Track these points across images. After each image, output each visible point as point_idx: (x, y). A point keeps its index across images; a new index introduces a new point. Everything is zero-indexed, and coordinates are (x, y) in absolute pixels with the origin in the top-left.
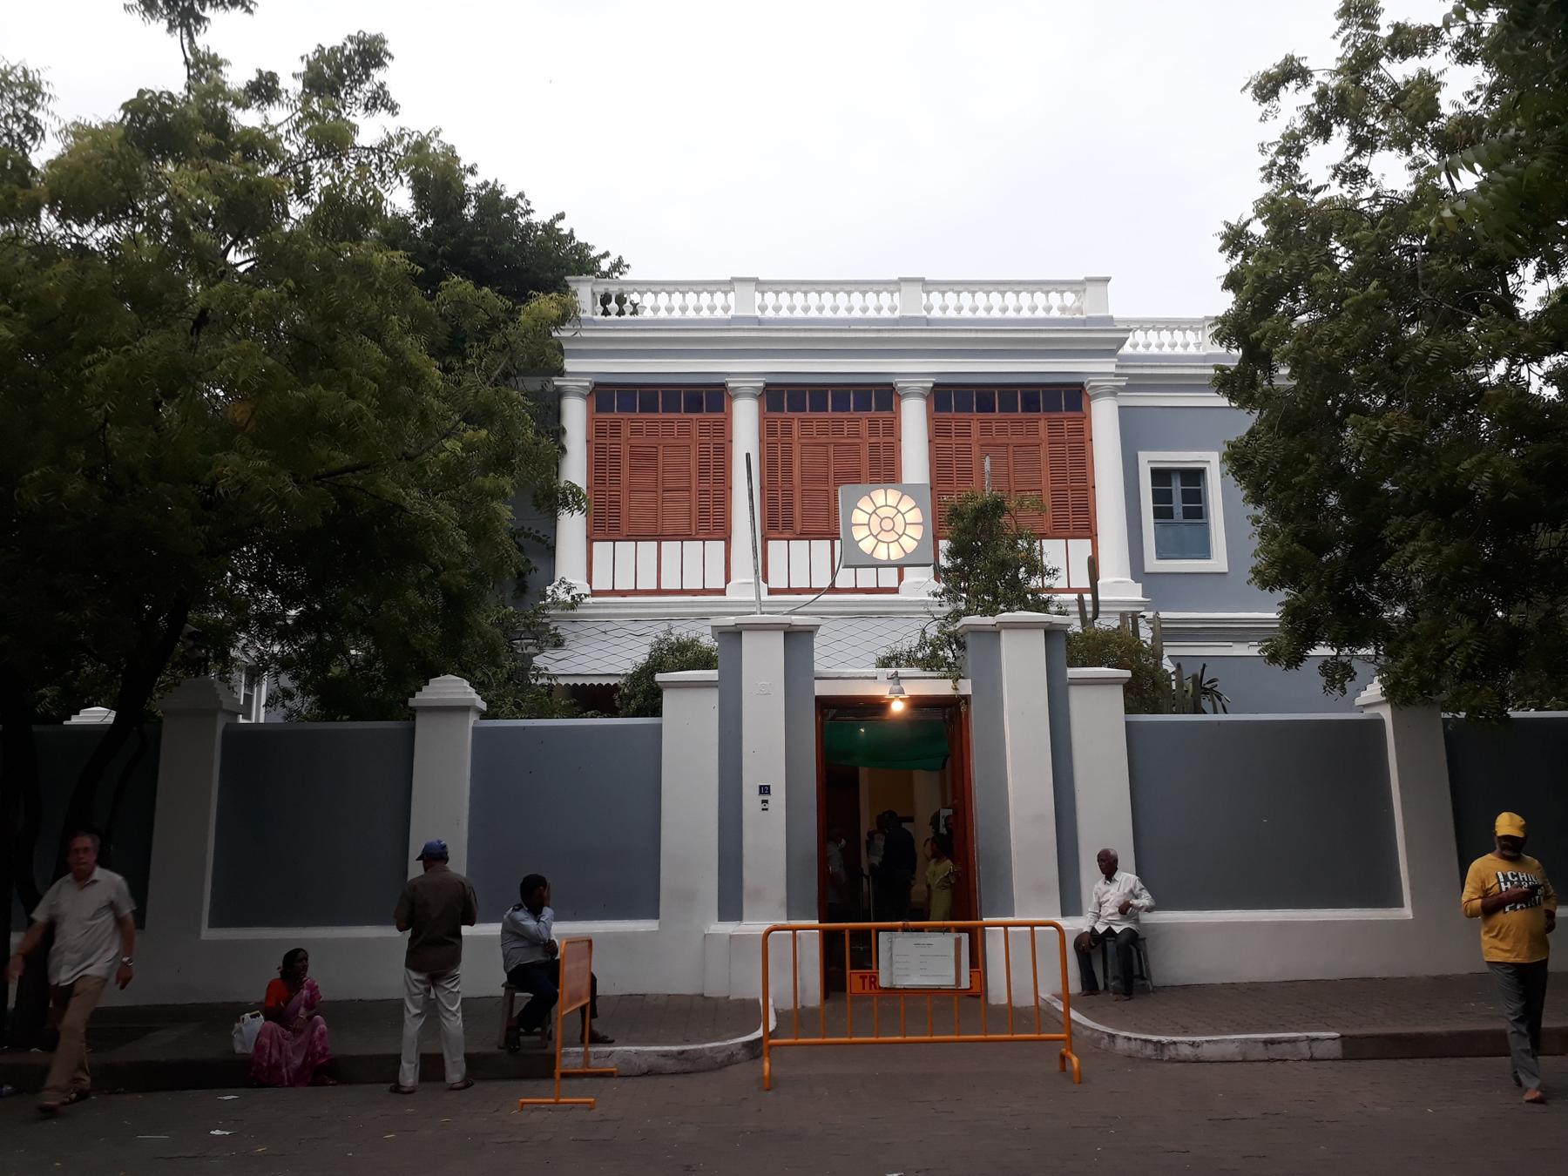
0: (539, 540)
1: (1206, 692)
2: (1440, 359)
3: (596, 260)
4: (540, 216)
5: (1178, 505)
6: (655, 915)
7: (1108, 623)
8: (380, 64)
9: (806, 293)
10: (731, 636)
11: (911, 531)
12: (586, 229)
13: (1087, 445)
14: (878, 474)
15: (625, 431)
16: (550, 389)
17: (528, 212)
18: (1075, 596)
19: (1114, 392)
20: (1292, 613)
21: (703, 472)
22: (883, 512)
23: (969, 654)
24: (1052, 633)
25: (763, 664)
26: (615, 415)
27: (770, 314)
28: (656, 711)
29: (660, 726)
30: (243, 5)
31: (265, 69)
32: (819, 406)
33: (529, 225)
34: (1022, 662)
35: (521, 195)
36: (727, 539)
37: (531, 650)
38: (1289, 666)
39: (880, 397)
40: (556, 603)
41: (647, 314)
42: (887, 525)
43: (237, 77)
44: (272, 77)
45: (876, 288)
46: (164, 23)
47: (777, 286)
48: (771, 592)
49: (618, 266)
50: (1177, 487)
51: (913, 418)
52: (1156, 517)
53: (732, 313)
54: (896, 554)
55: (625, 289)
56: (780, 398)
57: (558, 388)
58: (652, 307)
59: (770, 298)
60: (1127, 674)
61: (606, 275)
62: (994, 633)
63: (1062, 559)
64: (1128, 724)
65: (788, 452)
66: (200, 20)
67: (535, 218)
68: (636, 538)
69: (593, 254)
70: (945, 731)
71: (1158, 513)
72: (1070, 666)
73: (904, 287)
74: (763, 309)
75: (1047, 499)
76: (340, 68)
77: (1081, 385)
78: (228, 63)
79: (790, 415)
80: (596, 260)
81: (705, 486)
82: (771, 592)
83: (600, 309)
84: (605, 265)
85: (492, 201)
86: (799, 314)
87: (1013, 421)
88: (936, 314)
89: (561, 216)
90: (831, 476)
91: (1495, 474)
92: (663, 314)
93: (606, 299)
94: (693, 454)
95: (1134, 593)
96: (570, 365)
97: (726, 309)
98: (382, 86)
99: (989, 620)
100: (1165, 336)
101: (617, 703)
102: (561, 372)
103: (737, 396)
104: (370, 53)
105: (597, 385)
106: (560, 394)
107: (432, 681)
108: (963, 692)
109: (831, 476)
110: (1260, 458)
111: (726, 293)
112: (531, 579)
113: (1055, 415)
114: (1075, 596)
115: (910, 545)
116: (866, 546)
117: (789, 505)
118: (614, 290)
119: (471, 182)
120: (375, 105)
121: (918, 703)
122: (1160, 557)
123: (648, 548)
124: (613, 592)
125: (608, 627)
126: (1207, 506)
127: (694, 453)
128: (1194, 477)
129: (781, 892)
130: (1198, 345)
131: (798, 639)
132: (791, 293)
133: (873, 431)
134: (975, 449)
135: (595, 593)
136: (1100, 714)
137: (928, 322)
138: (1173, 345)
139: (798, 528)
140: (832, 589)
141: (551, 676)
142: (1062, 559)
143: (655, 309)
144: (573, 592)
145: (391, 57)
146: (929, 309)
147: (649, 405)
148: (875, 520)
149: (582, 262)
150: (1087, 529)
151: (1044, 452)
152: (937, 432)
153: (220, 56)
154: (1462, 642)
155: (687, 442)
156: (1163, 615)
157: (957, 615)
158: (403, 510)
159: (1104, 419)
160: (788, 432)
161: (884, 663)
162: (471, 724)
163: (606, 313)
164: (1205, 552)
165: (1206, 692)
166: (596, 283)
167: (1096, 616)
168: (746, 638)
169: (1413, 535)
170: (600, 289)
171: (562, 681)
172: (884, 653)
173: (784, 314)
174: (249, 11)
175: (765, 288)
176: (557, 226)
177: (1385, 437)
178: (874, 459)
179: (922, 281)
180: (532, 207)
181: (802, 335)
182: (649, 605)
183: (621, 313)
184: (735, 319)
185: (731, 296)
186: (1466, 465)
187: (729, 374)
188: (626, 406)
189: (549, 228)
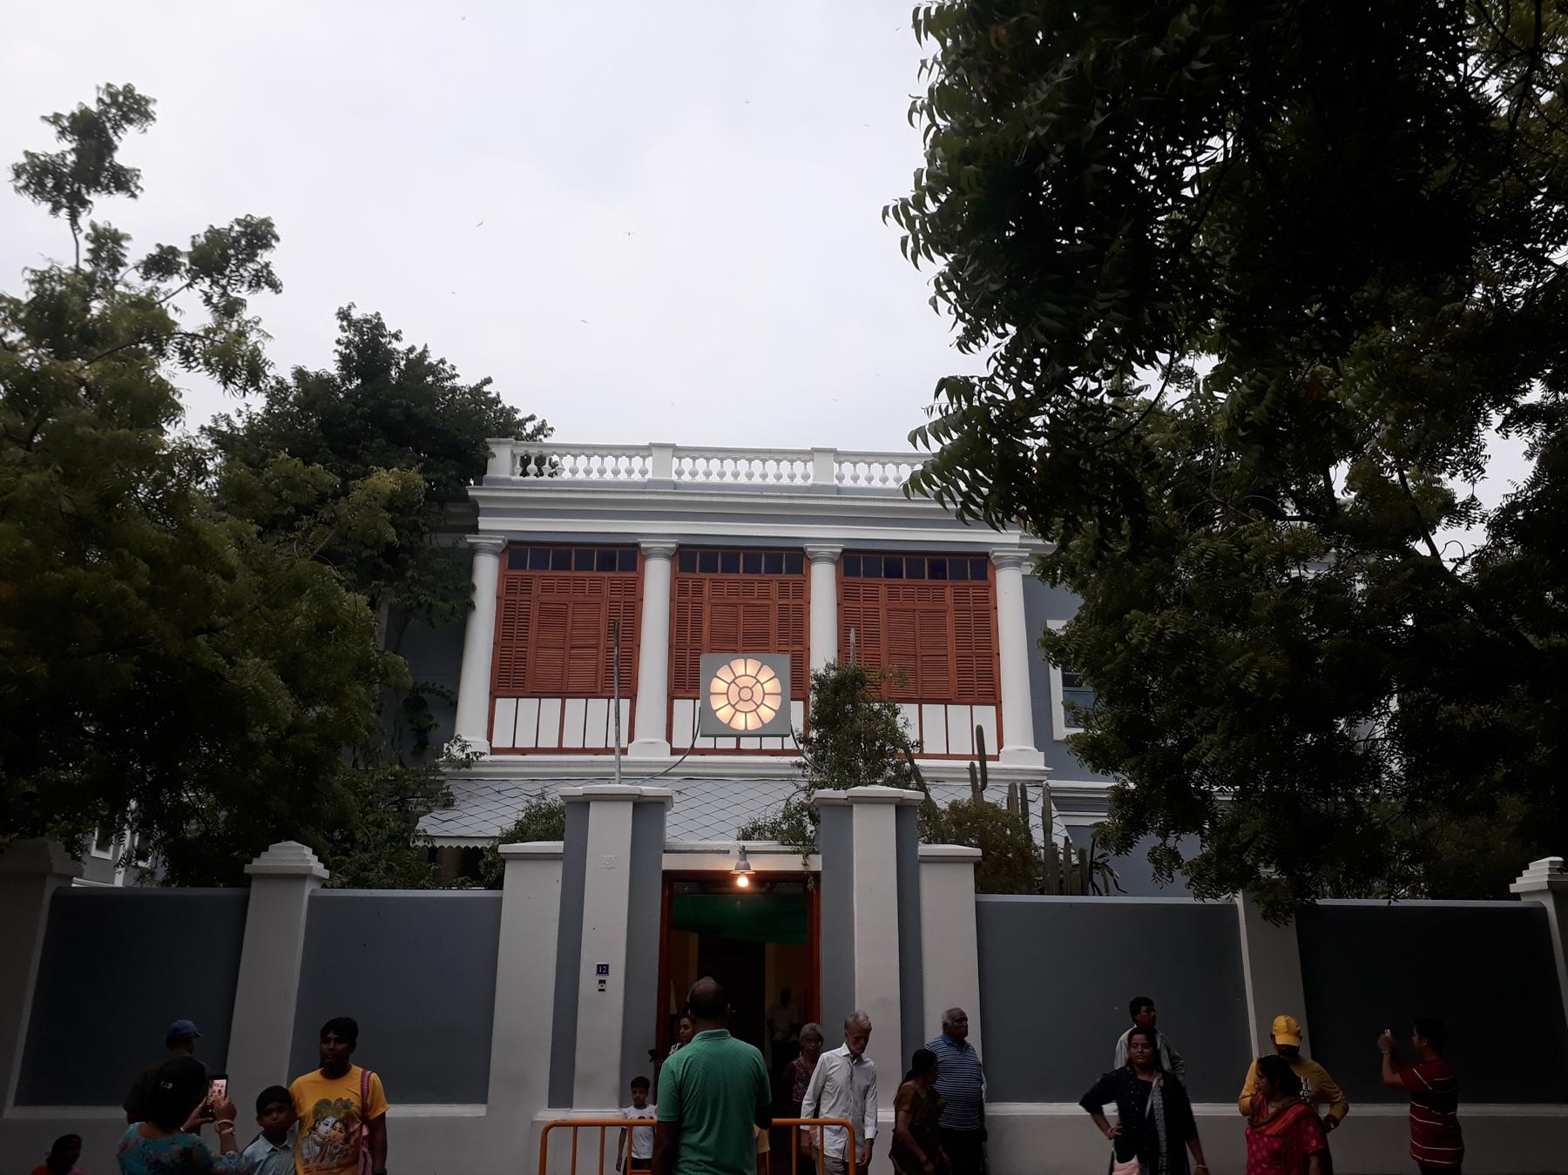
0: (443, 695)
1: (1098, 866)
2: (1214, 559)
3: (522, 423)
4: (466, 379)
6: (481, 1097)
7: (995, 796)
8: (267, 246)
9: (722, 460)
10: (582, 804)
11: (769, 701)
12: (512, 394)
14: (786, 635)
15: (536, 588)
16: (461, 545)
17: (453, 377)
18: (967, 763)
19: (1018, 563)
20: (1120, 795)
21: (613, 629)
22: (741, 682)
24: (902, 808)
25: (610, 835)
26: (527, 572)
27: (686, 478)
28: (498, 884)
29: (499, 900)
30: (129, 190)
31: (165, 244)
32: (731, 567)
33: (454, 390)
34: (873, 837)
35: (443, 361)
36: (633, 699)
37: (420, 809)
38: (1118, 853)
39: (794, 559)
40: (451, 761)
42: (746, 694)
43: (136, 251)
44: (173, 251)
45: (790, 457)
46: (49, 205)
47: (695, 452)
48: (674, 752)
49: (540, 430)
51: (823, 582)
53: (649, 476)
54: (752, 723)
55: (545, 451)
56: (691, 559)
57: (472, 545)
58: (571, 469)
60: (978, 852)
61: (531, 437)
62: (846, 807)
63: (937, 732)
65: (698, 613)
66: (85, 203)
67: (458, 382)
68: (540, 695)
69: (519, 417)
70: (794, 906)
74: (680, 473)
75: (952, 664)
76: (225, 248)
77: (986, 554)
78: (128, 238)
79: (703, 575)
80: (522, 423)
82: (674, 752)
83: (519, 469)
84: (529, 428)
85: (418, 365)
86: (714, 479)
87: (921, 587)
88: (848, 483)
89: (488, 381)
90: (740, 636)
91: (1262, 674)
92: (581, 476)
93: (525, 462)
95: (1037, 762)
96: (484, 523)
97: (643, 472)
98: (267, 265)
99: (842, 794)
101: (482, 871)
102: (475, 529)
104: (258, 235)
105: (511, 543)
106: (473, 551)
107: (273, 848)
109: (740, 636)
110: (1072, 645)
111: (644, 458)
112: (433, 735)
113: (962, 583)
114: (967, 763)
115: (767, 714)
116: (724, 714)
118: (534, 452)
119: (395, 345)
120: (258, 284)
121: (759, 879)
123: (552, 705)
124: (514, 750)
125: (503, 786)
129: (613, 1078)
131: (648, 811)
132: (708, 459)
133: (783, 593)
134: (883, 613)
135: (494, 751)
136: (951, 896)
137: (839, 490)
140: (738, 751)
141: (432, 838)
142: (937, 732)
143: (574, 471)
144: (468, 750)
145: (277, 239)
146: (840, 478)
147: (562, 563)
148: (734, 689)
149: (509, 426)
150: (992, 696)
151: (950, 619)
152: (845, 596)
153: (121, 231)
154: (1256, 834)
156: (1053, 783)
157: (814, 785)
158: (222, 677)
160: (699, 591)
161: (746, 836)
162: (307, 892)
163: (525, 473)
165: (1098, 866)
167: (984, 787)
168: (593, 807)
169: (1212, 729)
170: (521, 451)
171: (446, 844)
172: (745, 823)
173: (700, 478)
174: (134, 196)
176: (486, 389)
177: (1161, 633)
178: (783, 622)
181: (715, 499)
182: (548, 764)
184: (650, 481)
185: (649, 460)
186: (1237, 664)
188: (540, 563)
189: (477, 391)
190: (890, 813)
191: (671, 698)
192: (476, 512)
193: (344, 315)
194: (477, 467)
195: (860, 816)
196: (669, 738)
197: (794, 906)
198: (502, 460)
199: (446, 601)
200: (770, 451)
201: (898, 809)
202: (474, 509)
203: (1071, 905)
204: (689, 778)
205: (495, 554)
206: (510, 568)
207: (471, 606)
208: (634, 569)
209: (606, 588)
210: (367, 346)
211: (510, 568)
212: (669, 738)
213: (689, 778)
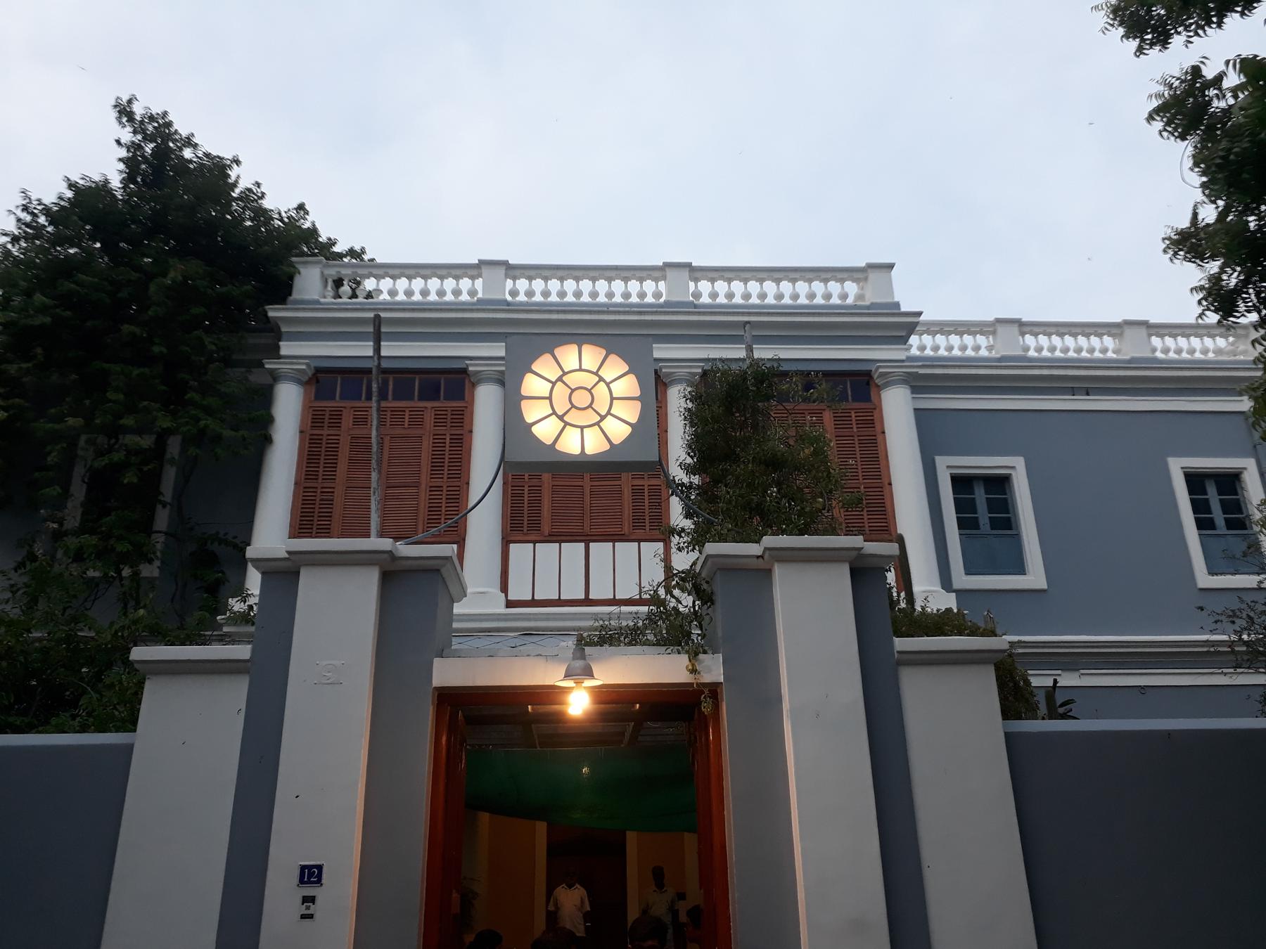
0: (235, 546)
11: (618, 409)
13: (879, 438)
21: (436, 467)
22: (574, 379)
23: (719, 613)
28: (130, 723)
29: (129, 749)
41: (385, 297)
42: (581, 399)
45: (638, 274)
48: (510, 604)
55: (360, 271)
59: (522, 284)
62: (759, 574)
64: (1008, 736)
71: (962, 524)
72: (900, 634)
73: (670, 273)
77: (868, 374)
81: (438, 482)
82: (510, 604)
88: (705, 299)
94: (425, 443)
96: (286, 348)
99: (753, 549)
100: (955, 340)
102: (274, 352)
103: (479, 382)
105: (318, 370)
106: (275, 377)
108: (707, 678)
113: (844, 405)
117: (536, 502)
122: (968, 572)
126: (1016, 515)
127: (427, 445)
128: (999, 484)
130: (990, 348)
139: (546, 529)
148: (560, 391)
159: (897, 409)
164: (1020, 569)
170: (332, 272)
175: (517, 273)
179: (688, 266)
181: (554, 316)
184: (479, 301)
185: (479, 283)
189: (292, 224)
190: (841, 578)
191: (506, 542)
192: (279, 336)
193: (124, 112)
194: (281, 290)
195: (784, 582)
196: (504, 588)
197: (670, 742)
198: (310, 282)
200: (616, 268)
201: (855, 573)
202: (274, 333)
203: (1169, 734)
204: (528, 633)
205: (299, 382)
206: (317, 398)
207: (267, 440)
209: (429, 418)
210: (160, 158)
211: (317, 398)
212: (504, 588)
213: (528, 633)
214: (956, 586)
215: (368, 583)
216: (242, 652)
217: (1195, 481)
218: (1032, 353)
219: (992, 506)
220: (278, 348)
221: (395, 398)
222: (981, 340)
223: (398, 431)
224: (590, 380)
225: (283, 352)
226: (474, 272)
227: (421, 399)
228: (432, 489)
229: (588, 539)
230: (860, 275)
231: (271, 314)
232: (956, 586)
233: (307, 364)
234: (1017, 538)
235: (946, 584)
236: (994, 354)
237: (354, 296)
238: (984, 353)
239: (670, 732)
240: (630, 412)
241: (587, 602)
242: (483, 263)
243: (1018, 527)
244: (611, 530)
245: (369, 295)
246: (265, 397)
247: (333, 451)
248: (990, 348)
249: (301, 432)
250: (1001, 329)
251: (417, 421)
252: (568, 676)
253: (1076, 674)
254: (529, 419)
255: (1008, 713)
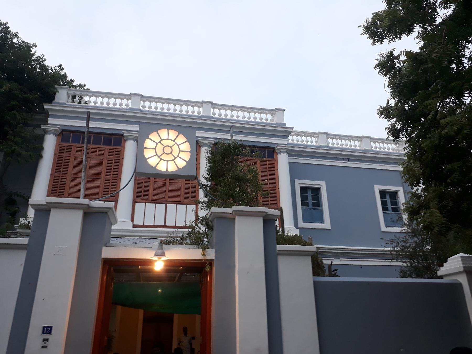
0: (24, 197)
5: (310, 201)
11: (182, 155)
12: (72, 73)
13: (276, 171)
21: (108, 171)
22: (165, 143)
23: (214, 234)
42: (168, 150)
45: (192, 104)
50: (310, 194)
52: (302, 205)
55: (83, 93)
59: (147, 104)
62: (230, 220)
64: (315, 283)
71: (303, 204)
73: (204, 105)
77: (273, 148)
81: (109, 177)
82: (134, 226)
83: (71, 101)
88: (217, 116)
96: (51, 121)
99: (229, 210)
102: (46, 122)
103: (127, 140)
105: (63, 131)
108: (208, 258)
113: (265, 159)
117: (147, 188)
122: (304, 221)
127: (105, 162)
128: (317, 190)
130: (316, 142)
138: (307, 142)
139: (151, 198)
148: (160, 146)
155: (102, 157)
159: (283, 162)
164: (322, 221)
166: (69, 90)
170: (72, 93)
175: (145, 99)
179: (211, 103)
180: (45, 57)
181: (159, 117)
183: (80, 102)
184: (130, 109)
185: (130, 102)
187: (125, 130)
189: (57, 73)
190: (260, 222)
191: (134, 202)
192: (48, 116)
194: (50, 98)
195: (240, 223)
196: (132, 220)
197: (193, 282)
198: (62, 95)
199: (27, 151)
202: (46, 115)
203: (368, 283)
206: (62, 141)
207: (41, 156)
208: (120, 145)
209: (106, 153)
211: (62, 141)
212: (132, 220)
214: (299, 226)
215: (78, 216)
216: (24, 241)
217: (383, 194)
218: (330, 145)
219: (313, 198)
220: (48, 120)
221: (93, 144)
222: (313, 139)
223: (94, 156)
224: (171, 143)
225: (49, 122)
226: (128, 97)
227: (104, 144)
228: (106, 180)
229: (166, 202)
230: (273, 112)
231: (45, 107)
232: (299, 226)
233: (59, 128)
234: (321, 211)
235: (296, 225)
236: (317, 145)
237: (80, 102)
238: (314, 144)
239: (194, 277)
240: (187, 157)
241: (165, 226)
242: (132, 94)
243: (322, 206)
244: (176, 200)
245: (86, 103)
246: (40, 140)
247: (67, 162)
248: (316, 142)
249: (55, 154)
250: (320, 136)
251: (102, 152)
252: (155, 255)
253: (339, 260)
254: (146, 156)
255: (315, 274)
